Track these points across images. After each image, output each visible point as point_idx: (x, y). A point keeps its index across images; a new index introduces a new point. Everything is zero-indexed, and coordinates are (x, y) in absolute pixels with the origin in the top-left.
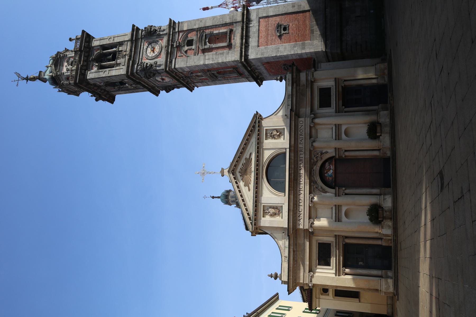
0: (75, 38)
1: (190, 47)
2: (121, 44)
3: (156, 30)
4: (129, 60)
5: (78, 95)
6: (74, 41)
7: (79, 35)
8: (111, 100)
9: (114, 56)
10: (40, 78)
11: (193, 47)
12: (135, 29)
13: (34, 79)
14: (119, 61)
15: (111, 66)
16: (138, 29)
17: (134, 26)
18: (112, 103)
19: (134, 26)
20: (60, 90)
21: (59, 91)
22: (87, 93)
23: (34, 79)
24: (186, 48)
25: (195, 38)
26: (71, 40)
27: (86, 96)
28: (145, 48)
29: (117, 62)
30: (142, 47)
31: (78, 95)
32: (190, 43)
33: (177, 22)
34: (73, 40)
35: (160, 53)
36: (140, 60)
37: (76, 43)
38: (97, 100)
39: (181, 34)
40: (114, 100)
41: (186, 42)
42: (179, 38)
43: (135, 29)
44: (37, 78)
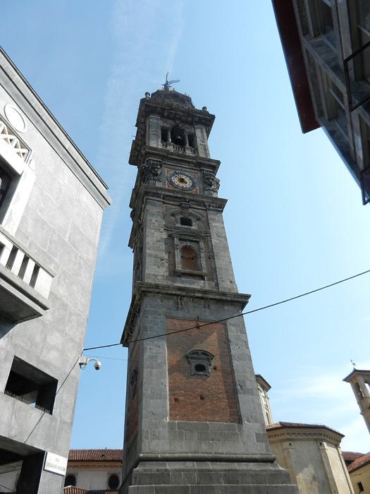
1: (179, 220)
2: (195, 150)
9: (179, 143)
11: (179, 225)
12: (215, 166)
24: (179, 217)
25: (193, 228)
28: (187, 174)
32: (186, 222)
42: (195, 211)
43: (215, 166)
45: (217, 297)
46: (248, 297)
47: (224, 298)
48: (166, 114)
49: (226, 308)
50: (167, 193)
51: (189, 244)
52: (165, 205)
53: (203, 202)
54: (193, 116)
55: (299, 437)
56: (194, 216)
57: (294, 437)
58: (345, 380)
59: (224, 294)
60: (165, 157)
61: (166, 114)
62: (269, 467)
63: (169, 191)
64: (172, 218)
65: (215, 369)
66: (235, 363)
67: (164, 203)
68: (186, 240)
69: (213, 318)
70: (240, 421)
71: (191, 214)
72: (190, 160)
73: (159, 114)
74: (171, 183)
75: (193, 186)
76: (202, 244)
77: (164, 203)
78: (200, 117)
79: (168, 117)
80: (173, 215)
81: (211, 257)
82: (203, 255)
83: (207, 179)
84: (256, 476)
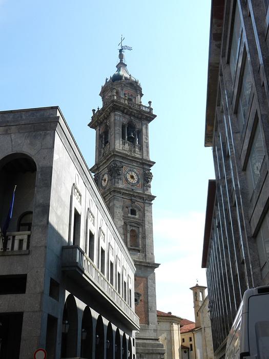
0: (152, 107)
2: (141, 149)
3: (148, 182)
4: (127, 155)
5: (100, 95)
6: (148, 105)
7: (154, 113)
8: (92, 125)
9: (132, 140)
10: (121, 65)
11: (130, 215)
13: (121, 56)
14: (127, 145)
15: (123, 138)
16: (151, 166)
17: (155, 163)
18: (89, 125)
19: (155, 163)
20: (108, 81)
21: (107, 79)
22: (101, 107)
23: (121, 56)
24: (130, 209)
25: (137, 217)
26: (150, 103)
27: (99, 104)
28: (135, 170)
29: (126, 142)
30: (136, 168)
31: (100, 95)
33: (153, 202)
34: (150, 105)
35: (129, 183)
36: (126, 165)
37: (146, 107)
38: (94, 111)
39: (143, 204)
40: (91, 127)
41: (135, 209)
42: (139, 204)
44: (121, 60)
45: (146, 265)
46: (158, 265)
47: (149, 265)
48: (125, 111)
49: (148, 269)
50: (125, 192)
52: (123, 199)
53: (143, 197)
54: (142, 115)
55: (163, 320)
56: (138, 208)
57: (161, 320)
58: (190, 289)
59: (149, 263)
60: (124, 157)
61: (125, 111)
62: (157, 342)
64: (126, 209)
65: (141, 300)
66: (149, 298)
67: (123, 198)
68: (133, 226)
69: (142, 275)
70: (148, 324)
71: (136, 207)
72: (138, 160)
73: (121, 111)
74: (127, 180)
75: (138, 182)
76: (141, 229)
77: (123, 198)
78: (147, 116)
79: (126, 114)
80: (127, 207)
81: (144, 238)
82: (140, 236)
83: (147, 178)
84: (152, 345)
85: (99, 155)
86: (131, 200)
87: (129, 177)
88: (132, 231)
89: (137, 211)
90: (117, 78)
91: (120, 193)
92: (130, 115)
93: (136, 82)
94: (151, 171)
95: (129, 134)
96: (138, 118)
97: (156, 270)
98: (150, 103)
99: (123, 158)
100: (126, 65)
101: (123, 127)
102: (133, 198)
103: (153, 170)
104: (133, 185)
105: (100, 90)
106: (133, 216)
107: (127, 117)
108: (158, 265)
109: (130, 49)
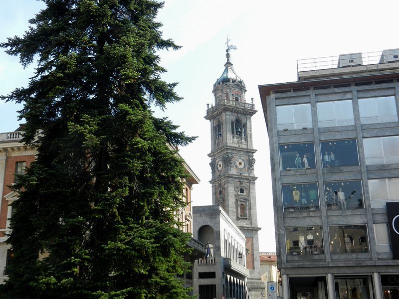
0: (254, 103)
2: (246, 140)
5: (213, 92)
9: (239, 134)
10: (228, 64)
11: (239, 193)
12: (254, 151)
13: (228, 56)
23: (228, 56)
24: (239, 189)
25: (244, 194)
26: (252, 99)
31: (213, 92)
34: (252, 101)
43: (254, 151)
44: (228, 60)
46: (260, 229)
48: (234, 110)
51: (243, 203)
59: (254, 228)
60: (234, 149)
61: (234, 110)
62: (260, 281)
63: (236, 175)
70: (254, 269)
74: (236, 166)
75: (245, 167)
76: (247, 203)
79: (235, 112)
81: (250, 209)
82: (247, 208)
84: (257, 283)
85: (215, 144)
86: (240, 182)
87: (238, 164)
88: (241, 204)
89: (244, 189)
90: (225, 81)
91: (232, 177)
92: (238, 112)
93: (241, 82)
94: (254, 157)
95: (237, 129)
96: (243, 114)
97: (259, 232)
98: (252, 99)
99: (233, 150)
100: (232, 64)
101: (232, 123)
102: (241, 180)
103: (255, 156)
104: (241, 170)
105: (212, 88)
106: (242, 194)
107: (235, 114)
108: (260, 229)
109: (235, 49)
